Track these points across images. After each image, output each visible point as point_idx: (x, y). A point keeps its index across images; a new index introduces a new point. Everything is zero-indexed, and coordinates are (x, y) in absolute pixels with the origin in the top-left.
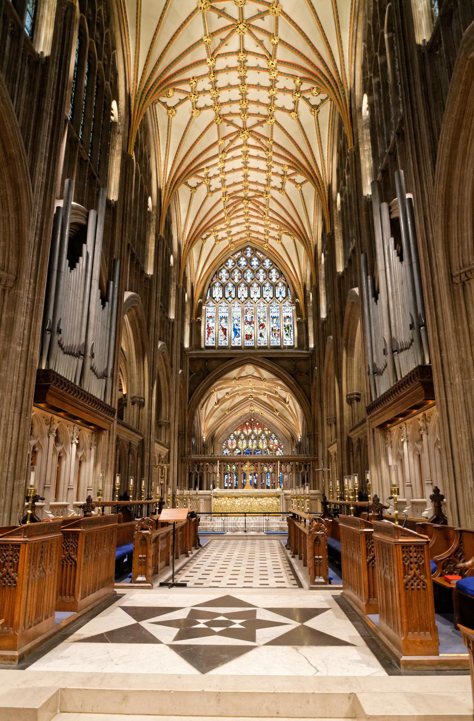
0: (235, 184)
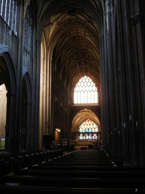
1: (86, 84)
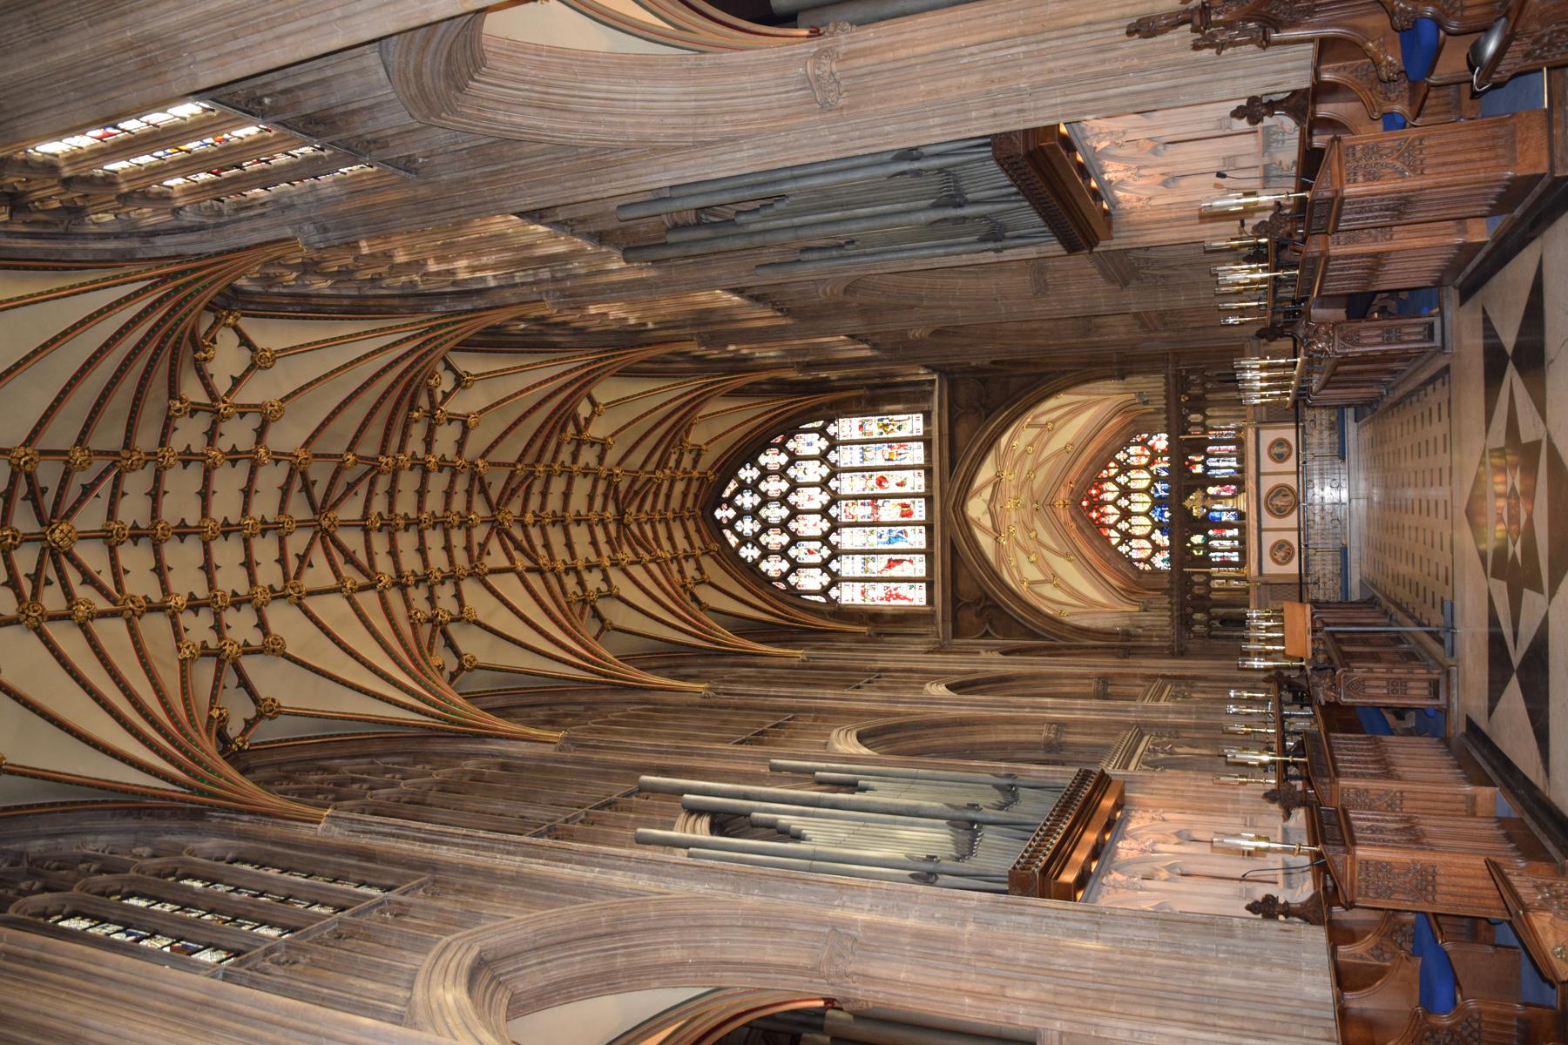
0: (594, 543)
1: (775, 513)
